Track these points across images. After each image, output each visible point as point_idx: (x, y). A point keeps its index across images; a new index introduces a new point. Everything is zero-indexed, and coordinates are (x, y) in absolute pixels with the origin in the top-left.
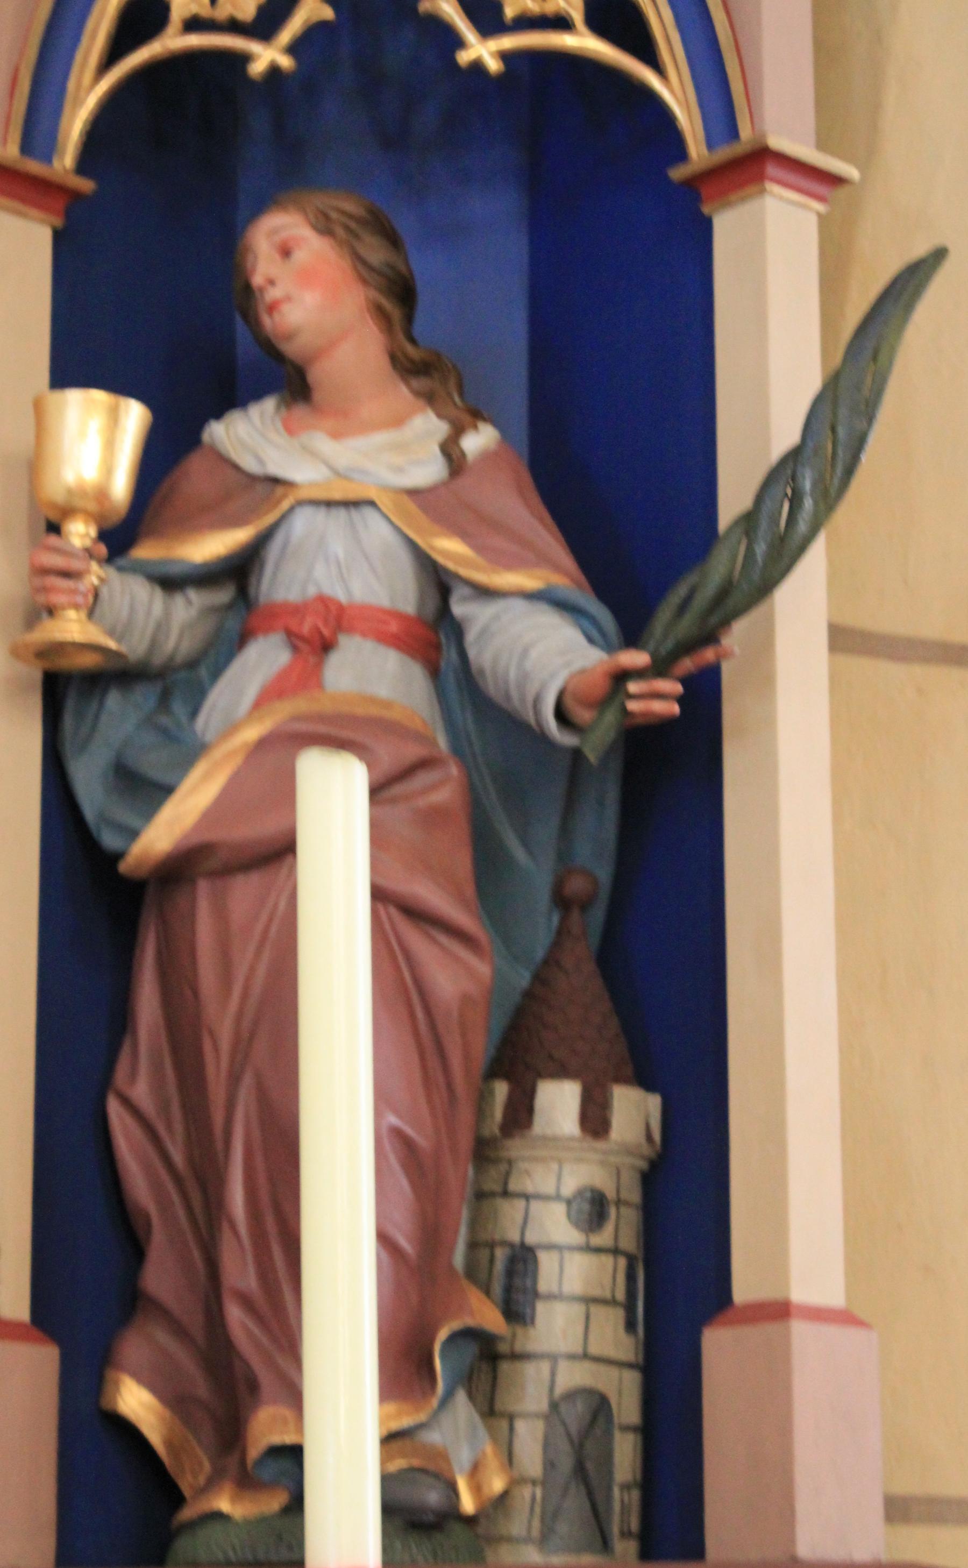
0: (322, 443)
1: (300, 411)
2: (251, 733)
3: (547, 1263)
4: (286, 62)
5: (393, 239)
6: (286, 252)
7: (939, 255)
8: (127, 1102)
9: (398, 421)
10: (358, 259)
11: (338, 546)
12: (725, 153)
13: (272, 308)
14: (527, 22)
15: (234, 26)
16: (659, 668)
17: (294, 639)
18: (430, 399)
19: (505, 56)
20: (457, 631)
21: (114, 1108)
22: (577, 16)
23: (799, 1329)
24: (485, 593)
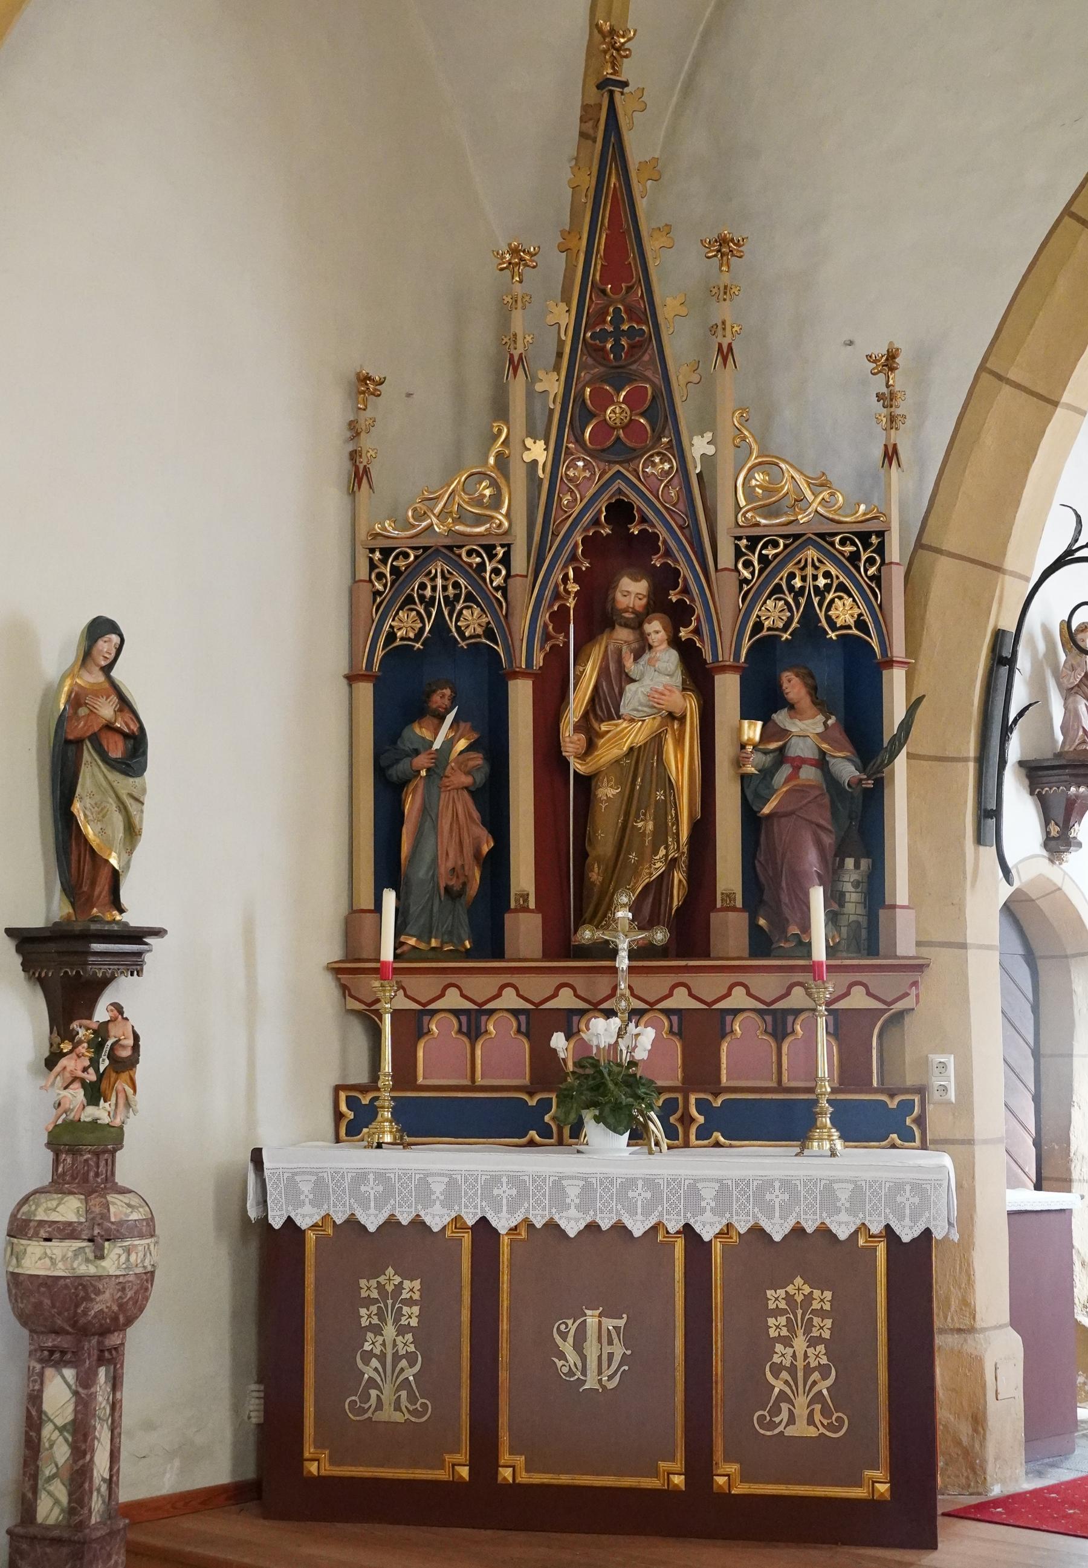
0: (797, 721)
1: (792, 712)
2: (785, 789)
3: (847, 895)
4: (789, 637)
5: (812, 677)
6: (789, 681)
7: (924, 696)
8: (759, 861)
9: (814, 717)
10: (805, 683)
11: (801, 745)
12: (883, 660)
13: (787, 694)
14: (843, 627)
15: (777, 629)
16: (868, 779)
17: (792, 766)
18: (822, 712)
19: (837, 636)
20: (827, 762)
21: (756, 862)
22: (853, 626)
23: (897, 910)
24: (834, 757)
